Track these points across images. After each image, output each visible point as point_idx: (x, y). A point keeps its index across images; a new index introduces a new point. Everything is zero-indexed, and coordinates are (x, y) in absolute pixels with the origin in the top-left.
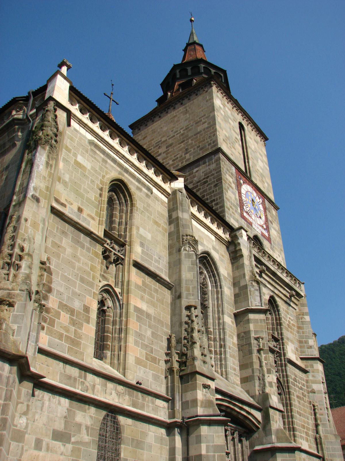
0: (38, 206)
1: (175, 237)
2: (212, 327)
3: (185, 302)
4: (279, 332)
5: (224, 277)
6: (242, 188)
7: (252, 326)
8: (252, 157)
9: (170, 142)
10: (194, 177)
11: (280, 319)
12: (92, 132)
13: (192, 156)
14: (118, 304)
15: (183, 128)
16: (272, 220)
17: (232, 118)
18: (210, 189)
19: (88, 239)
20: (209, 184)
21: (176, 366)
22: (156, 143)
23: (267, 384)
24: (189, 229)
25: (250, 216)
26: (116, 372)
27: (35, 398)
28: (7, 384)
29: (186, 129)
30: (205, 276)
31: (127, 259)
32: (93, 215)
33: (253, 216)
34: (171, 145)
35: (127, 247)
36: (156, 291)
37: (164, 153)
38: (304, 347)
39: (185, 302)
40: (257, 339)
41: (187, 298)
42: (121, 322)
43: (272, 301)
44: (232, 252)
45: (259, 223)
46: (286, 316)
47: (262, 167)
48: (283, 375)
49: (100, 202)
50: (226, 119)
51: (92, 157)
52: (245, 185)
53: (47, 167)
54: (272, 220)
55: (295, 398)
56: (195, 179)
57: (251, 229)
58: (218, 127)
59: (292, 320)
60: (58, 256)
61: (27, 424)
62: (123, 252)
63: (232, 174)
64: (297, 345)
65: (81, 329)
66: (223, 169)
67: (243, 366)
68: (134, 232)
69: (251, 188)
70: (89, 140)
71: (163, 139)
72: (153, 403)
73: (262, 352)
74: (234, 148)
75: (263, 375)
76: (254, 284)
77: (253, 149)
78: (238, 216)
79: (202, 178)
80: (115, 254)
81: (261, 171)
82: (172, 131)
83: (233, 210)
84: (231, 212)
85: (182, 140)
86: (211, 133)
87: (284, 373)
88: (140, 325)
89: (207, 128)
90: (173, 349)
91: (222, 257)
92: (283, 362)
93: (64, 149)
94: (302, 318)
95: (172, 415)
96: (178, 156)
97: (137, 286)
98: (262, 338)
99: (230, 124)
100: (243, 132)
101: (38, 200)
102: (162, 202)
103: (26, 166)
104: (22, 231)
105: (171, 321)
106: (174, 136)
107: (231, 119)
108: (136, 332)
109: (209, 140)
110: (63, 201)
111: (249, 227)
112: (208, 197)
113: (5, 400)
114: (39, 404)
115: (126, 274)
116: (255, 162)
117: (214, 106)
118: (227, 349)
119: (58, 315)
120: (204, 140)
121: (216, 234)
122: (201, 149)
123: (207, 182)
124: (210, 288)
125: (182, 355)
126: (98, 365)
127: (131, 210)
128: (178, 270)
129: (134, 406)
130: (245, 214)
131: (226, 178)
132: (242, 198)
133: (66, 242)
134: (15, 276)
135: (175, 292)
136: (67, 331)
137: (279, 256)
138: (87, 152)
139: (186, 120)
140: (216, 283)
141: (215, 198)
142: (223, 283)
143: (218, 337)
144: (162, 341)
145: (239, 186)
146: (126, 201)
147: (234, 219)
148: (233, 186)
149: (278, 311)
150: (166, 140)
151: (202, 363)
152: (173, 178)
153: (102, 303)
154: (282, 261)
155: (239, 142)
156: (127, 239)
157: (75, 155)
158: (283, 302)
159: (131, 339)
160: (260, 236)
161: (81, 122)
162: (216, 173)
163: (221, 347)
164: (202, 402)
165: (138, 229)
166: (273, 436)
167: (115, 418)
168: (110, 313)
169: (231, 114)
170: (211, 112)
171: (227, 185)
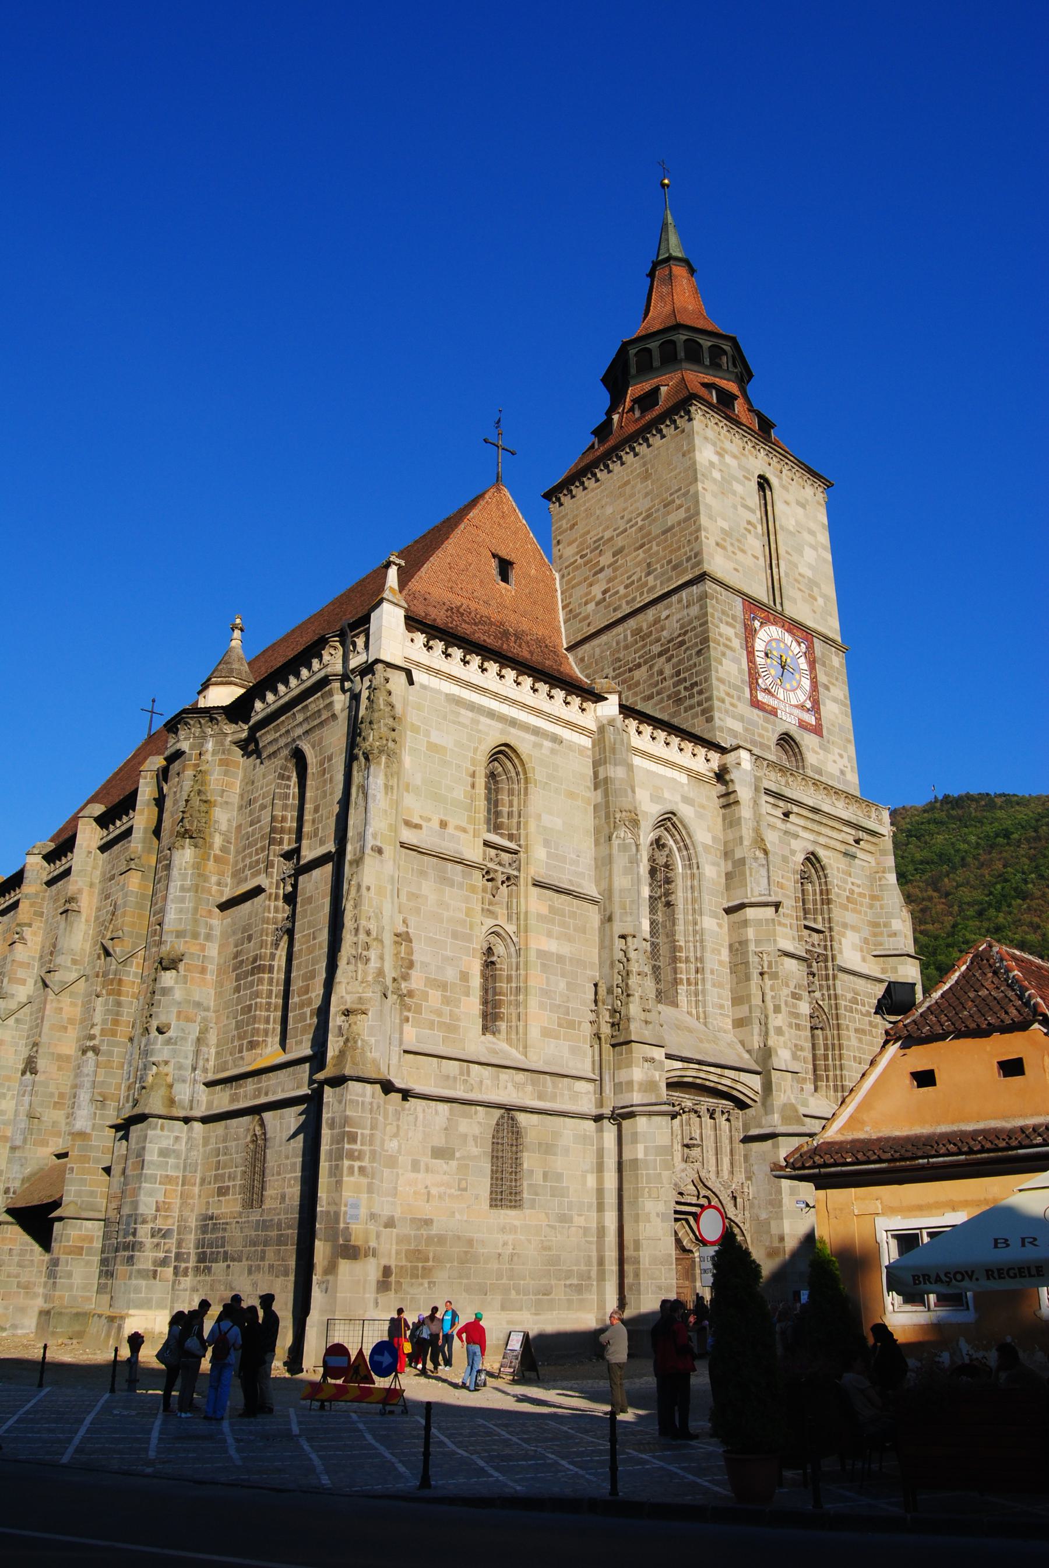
0: (382, 861)
1: (603, 814)
2: (682, 938)
3: (618, 928)
4: (826, 916)
5: (706, 847)
6: (757, 640)
7: (751, 933)
8: (787, 552)
9: (620, 544)
10: (663, 629)
11: (828, 892)
12: (450, 677)
13: (658, 582)
14: (513, 949)
15: (641, 513)
16: (830, 682)
17: (740, 474)
18: (690, 658)
19: (459, 867)
20: (687, 649)
21: (606, 1030)
22: (595, 542)
23: (772, 1032)
24: (627, 797)
25: (773, 695)
26: (513, 1051)
27: (407, 1112)
28: (371, 1111)
29: (648, 516)
30: (670, 850)
31: (522, 875)
32: (464, 824)
33: (781, 691)
35: (522, 855)
36: (573, 915)
37: (609, 567)
38: (881, 934)
39: (618, 928)
40: (759, 954)
41: (621, 921)
42: (518, 976)
43: (812, 859)
44: (722, 796)
45: (794, 702)
46: (845, 882)
47: (814, 563)
48: (829, 996)
49: (472, 799)
50: (725, 489)
51: (454, 722)
52: (766, 628)
53: (386, 793)
54: (830, 682)
55: (852, 1034)
56: (665, 633)
57: (774, 724)
58: (704, 520)
59: (859, 886)
60: (418, 911)
61: (400, 1147)
62: (515, 865)
63: (734, 618)
64: (866, 932)
65: (458, 1007)
66: (713, 616)
67: (738, 1000)
68: (532, 827)
69: (780, 630)
70: (447, 695)
71: (607, 535)
72: (570, 1089)
73: (766, 976)
74: (743, 551)
75: (766, 1017)
76: (760, 854)
77: (792, 529)
78: (745, 709)
79: (676, 634)
80: (503, 873)
81: (809, 573)
83: (732, 697)
84: (728, 706)
86: (691, 534)
87: (832, 992)
88: (547, 978)
89: (686, 520)
90: (600, 1004)
91: (701, 810)
92: (831, 972)
93: (408, 732)
94: (880, 879)
95: (600, 1104)
96: (635, 578)
97: (540, 917)
98: (768, 954)
99: (734, 493)
100: (768, 493)
101: (380, 851)
102: (581, 750)
103: (358, 791)
104: (365, 907)
105: (600, 957)
106: (625, 530)
108: (541, 989)
109: (687, 549)
110: (416, 820)
111: (766, 721)
112: (687, 674)
113: (371, 1129)
114: (411, 1118)
115: (522, 900)
116: (795, 558)
117: (695, 470)
118: (708, 975)
119: (425, 996)
120: (679, 548)
121: (688, 771)
122: (674, 568)
123: (682, 643)
124: (680, 870)
125: (614, 1011)
126: (487, 1048)
127: (526, 789)
128: (607, 873)
129: (540, 1098)
130: (761, 696)
131: (720, 635)
132: (754, 663)
133: (428, 888)
134: (365, 972)
135: (605, 910)
136: (439, 1013)
137: (841, 756)
138: (445, 718)
139: (647, 495)
140: (690, 859)
141: (698, 679)
142: (702, 860)
143: (692, 954)
144: (585, 993)
145: (750, 634)
146: (517, 774)
147: (733, 717)
148: (737, 643)
149: (826, 877)
150: (611, 539)
151: (643, 1024)
152: (599, 698)
153: (490, 951)
154: (849, 765)
155: (755, 527)
156: (522, 842)
157: (427, 734)
158: (840, 856)
159: (533, 1003)
161: (429, 670)
162: (701, 625)
163: (697, 972)
164: (641, 1084)
165: (539, 817)
166: (776, 1116)
167: (513, 1119)
168: (504, 967)
169: (741, 467)
170: (691, 484)
171: (721, 648)
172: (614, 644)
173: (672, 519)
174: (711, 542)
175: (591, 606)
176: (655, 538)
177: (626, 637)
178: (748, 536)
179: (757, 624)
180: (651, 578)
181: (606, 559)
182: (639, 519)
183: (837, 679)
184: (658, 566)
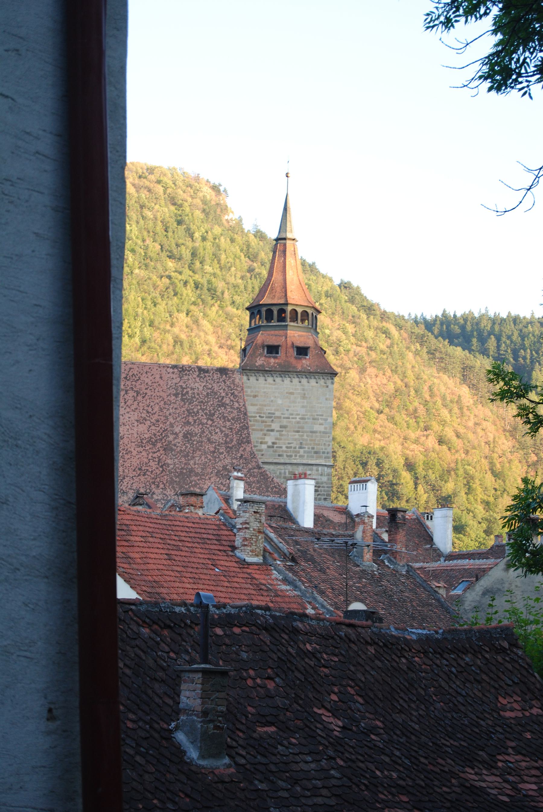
22: (269, 413)
34: (285, 427)
37: (277, 431)
71: (278, 414)
82: (288, 410)
85: (297, 429)
89: (324, 433)
106: (289, 418)
122: (316, 453)
150: (280, 417)
172: (278, 473)
173: (317, 428)
175: (264, 447)
176: (306, 432)
177: (285, 473)
180: (302, 451)
181: (275, 426)
182: (298, 417)
184: (307, 447)
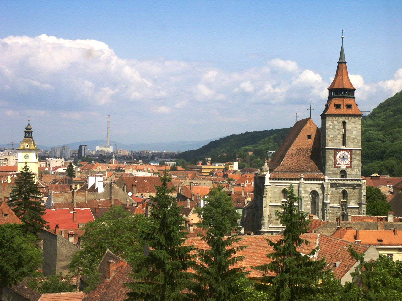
32: (278, 200)
45: (345, 163)
52: (340, 152)
58: (327, 137)
74: (335, 139)
77: (350, 129)
78: (332, 169)
81: (354, 137)
99: (335, 128)
107: (336, 125)
111: (337, 169)
130: (337, 165)
137: (356, 170)
145: (336, 154)
147: (330, 171)
148: (332, 158)
160: (344, 169)
174: (328, 141)
178: (338, 136)
179: (338, 152)
183: (358, 156)
